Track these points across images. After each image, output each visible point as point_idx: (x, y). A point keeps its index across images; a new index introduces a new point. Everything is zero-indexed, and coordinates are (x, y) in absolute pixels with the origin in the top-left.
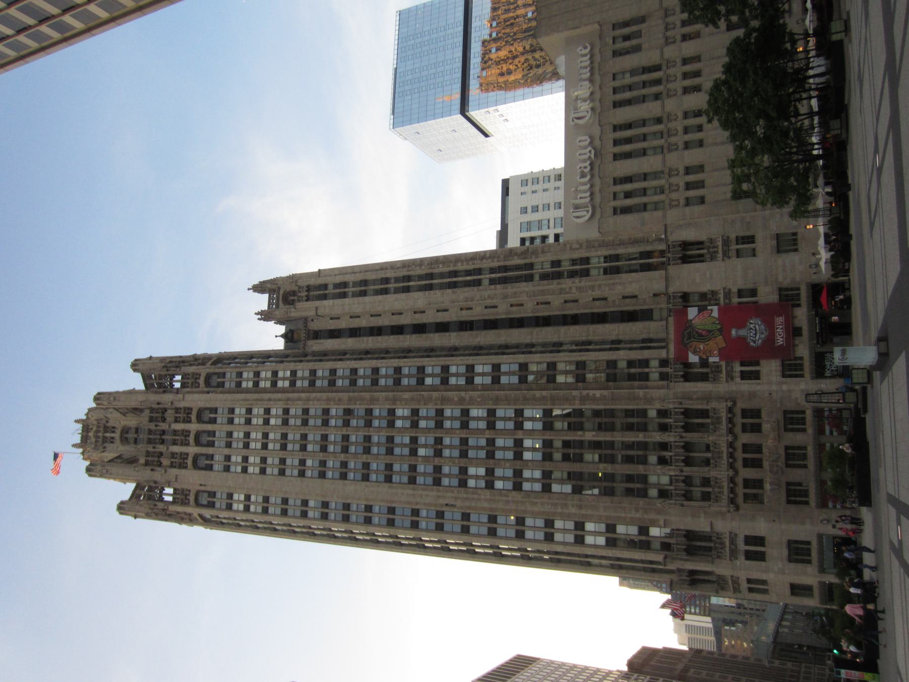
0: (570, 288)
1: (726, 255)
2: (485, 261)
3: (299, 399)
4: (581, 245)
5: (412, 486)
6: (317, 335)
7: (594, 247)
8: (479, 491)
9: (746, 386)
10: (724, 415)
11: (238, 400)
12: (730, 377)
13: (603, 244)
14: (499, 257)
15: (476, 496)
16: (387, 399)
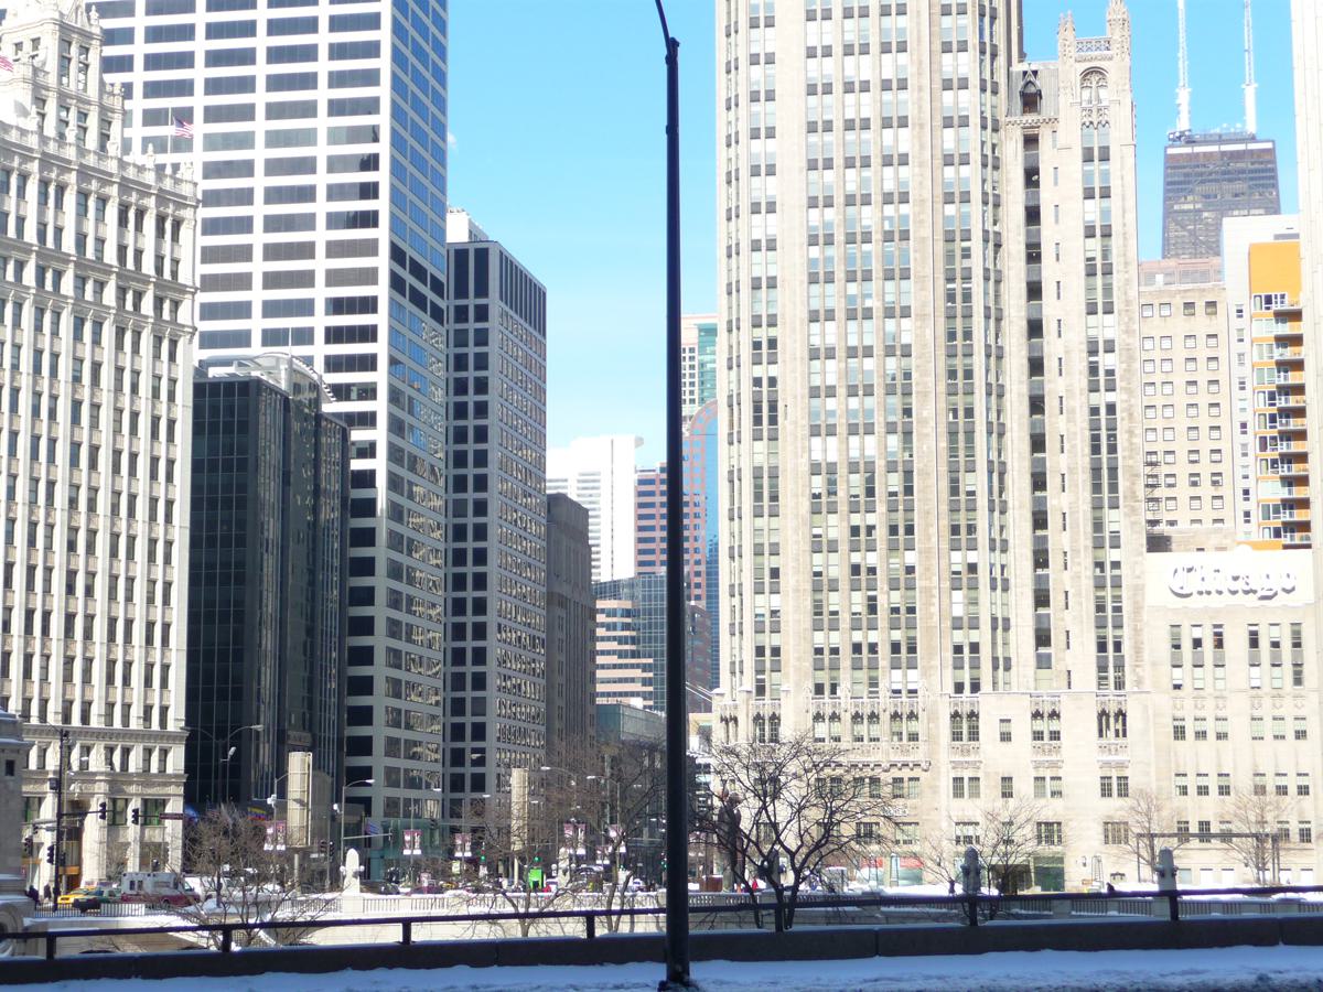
0: (1079, 564)
1: (1107, 764)
2: (1126, 436)
3: (922, 147)
4: (1139, 577)
5: (807, 357)
6: (1031, 141)
7: (1135, 595)
8: (806, 455)
9: (946, 785)
10: (910, 759)
11: (918, 24)
12: (956, 765)
13: (1138, 609)
14: (1131, 457)
15: (800, 450)
16: (924, 305)
